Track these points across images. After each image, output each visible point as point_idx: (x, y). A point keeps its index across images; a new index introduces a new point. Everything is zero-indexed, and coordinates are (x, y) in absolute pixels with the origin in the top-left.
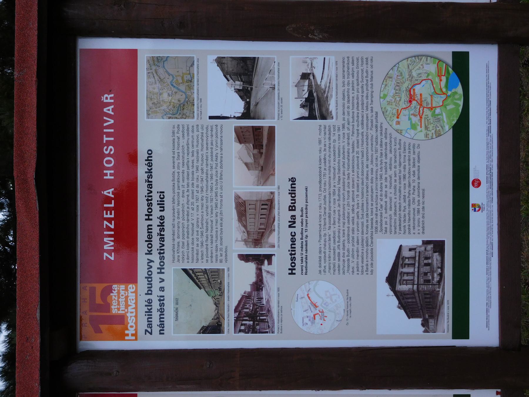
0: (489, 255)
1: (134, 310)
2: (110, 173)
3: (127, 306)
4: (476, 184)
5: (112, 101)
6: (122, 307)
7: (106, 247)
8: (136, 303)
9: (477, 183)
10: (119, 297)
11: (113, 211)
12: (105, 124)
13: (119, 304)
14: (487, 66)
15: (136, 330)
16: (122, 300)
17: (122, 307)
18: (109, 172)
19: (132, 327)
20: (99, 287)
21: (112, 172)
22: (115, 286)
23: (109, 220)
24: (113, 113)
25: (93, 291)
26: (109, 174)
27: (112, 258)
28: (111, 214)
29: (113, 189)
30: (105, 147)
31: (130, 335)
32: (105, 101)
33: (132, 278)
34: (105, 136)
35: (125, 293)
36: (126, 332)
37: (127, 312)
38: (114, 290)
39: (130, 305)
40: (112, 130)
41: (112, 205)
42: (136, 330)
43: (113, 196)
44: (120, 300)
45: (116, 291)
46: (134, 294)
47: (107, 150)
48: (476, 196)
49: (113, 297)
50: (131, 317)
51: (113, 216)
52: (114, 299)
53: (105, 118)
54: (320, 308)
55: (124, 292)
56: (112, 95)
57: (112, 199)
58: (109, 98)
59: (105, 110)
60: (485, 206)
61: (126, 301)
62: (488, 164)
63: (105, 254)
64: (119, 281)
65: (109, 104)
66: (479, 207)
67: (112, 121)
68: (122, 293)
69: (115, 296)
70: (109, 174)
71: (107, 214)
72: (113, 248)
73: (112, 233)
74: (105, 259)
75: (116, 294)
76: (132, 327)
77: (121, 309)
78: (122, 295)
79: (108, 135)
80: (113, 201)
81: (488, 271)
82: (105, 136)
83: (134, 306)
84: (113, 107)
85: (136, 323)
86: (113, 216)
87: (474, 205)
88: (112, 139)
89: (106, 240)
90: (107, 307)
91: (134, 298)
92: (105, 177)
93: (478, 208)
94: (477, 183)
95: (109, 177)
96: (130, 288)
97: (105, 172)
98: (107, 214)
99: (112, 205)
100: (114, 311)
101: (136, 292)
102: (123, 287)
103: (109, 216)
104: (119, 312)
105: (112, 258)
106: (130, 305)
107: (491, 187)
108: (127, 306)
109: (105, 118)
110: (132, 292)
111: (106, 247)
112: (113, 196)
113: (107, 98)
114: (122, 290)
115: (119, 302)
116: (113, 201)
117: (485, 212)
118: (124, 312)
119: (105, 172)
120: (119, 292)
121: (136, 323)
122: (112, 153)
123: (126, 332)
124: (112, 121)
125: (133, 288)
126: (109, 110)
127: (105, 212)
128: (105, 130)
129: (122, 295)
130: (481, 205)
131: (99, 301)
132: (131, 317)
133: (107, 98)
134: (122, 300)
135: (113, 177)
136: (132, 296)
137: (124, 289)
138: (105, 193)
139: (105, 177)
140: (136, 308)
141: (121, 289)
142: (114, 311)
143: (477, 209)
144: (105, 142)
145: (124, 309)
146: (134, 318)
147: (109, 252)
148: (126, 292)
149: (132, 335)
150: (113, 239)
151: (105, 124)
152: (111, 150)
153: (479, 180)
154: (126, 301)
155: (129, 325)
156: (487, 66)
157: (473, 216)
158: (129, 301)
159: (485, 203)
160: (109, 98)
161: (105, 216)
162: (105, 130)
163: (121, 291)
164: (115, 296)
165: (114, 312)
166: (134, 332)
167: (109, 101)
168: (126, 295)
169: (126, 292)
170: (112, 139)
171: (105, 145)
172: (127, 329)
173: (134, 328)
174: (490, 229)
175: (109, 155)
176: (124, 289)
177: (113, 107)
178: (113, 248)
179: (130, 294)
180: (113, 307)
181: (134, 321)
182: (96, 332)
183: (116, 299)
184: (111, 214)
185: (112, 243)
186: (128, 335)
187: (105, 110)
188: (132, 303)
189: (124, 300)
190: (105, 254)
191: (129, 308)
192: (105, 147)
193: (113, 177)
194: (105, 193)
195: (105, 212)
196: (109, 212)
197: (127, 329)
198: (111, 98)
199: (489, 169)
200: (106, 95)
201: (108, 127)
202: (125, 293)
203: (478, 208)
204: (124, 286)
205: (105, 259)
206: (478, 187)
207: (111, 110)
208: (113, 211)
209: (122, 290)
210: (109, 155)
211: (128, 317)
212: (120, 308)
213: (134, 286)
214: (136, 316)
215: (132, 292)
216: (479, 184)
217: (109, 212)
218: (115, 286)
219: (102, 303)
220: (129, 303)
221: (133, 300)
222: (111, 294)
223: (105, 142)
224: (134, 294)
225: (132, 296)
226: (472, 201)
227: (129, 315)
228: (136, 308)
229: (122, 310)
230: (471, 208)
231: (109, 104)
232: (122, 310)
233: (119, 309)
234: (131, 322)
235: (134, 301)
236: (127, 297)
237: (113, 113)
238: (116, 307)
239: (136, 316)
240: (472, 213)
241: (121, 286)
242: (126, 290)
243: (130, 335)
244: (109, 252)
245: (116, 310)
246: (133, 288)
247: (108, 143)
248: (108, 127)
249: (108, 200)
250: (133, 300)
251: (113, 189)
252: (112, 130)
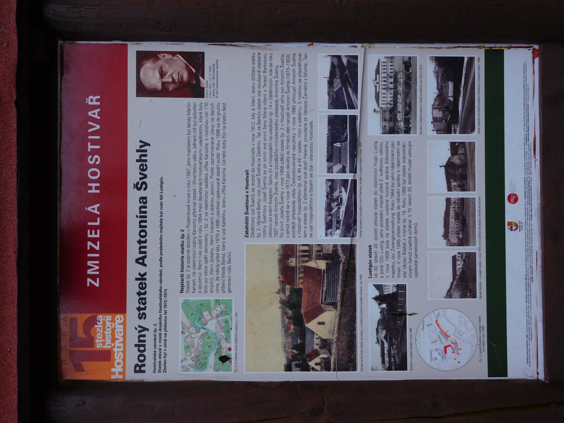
0: (529, 280)
1: (122, 345)
2: (95, 187)
3: (114, 340)
4: (512, 199)
5: (98, 103)
6: (108, 341)
7: (89, 272)
8: (124, 337)
9: (514, 199)
10: (104, 330)
11: (98, 231)
12: (90, 130)
13: (104, 338)
14: (525, 66)
15: (124, 367)
17: (108, 341)
18: (94, 185)
19: (119, 364)
20: (82, 318)
21: (98, 185)
23: (94, 241)
24: (99, 118)
25: (73, 321)
26: (94, 188)
27: (97, 285)
28: (96, 233)
29: (98, 205)
30: (90, 157)
31: (117, 373)
32: (90, 103)
33: (121, 308)
34: (89, 143)
35: (112, 325)
36: (113, 370)
37: (114, 347)
38: (99, 321)
39: (118, 339)
40: (98, 137)
41: (98, 223)
42: (124, 367)
43: (98, 213)
44: (106, 333)
45: (101, 323)
46: (122, 326)
47: (91, 160)
48: (512, 212)
49: (98, 329)
50: (118, 352)
51: (98, 236)
52: (99, 332)
53: (90, 123)
54: (453, 338)
55: (110, 323)
56: (98, 97)
57: (97, 216)
58: (94, 100)
59: (90, 114)
60: (524, 224)
61: (113, 334)
62: (526, 176)
63: (89, 280)
65: (95, 107)
66: (516, 225)
67: (98, 127)
68: (108, 324)
69: (100, 328)
70: (94, 188)
71: (91, 233)
72: (97, 273)
73: (98, 255)
74: (88, 285)
75: (102, 326)
76: (119, 364)
77: (106, 344)
78: (108, 328)
79: (94, 142)
80: (98, 219)
81: (528, 298)
82: (89, 143)
83: (122, 340)
84: (99, 110)
85: (124, 360)
86: (98, 236)
87: (509, 224)
88: (98, 147)
89: (89, 263)
90: (91, 341)
91: (122, 330)
92: (90, 191)
93: (515, 226)
94: (514, 199)
95: (94, 191)
96: (118, 319)
97: (90, 185)
98: (91, 233)
99: (98, 223)
100: (99, 346)
101: (124, 324)
102: (109, 317)
103: (93, 236)
104: (104, 347)
105: (97, 285)
106: (118, 339)
107: (530, 203)
108: (114, 340)
109: (90, 123)
110: (119, 324)
111: (89, 272)
112: (98, 213)
113: (93, 100)
114: (109, 321)
115: (104, 335)
116: (98, 219)
117: (523, 232)
118: (110, 347)
119: (90, 185)
120: (104, 324)
121: (124, 360)
122: (98, 163)
123: (113, 370)
124: (98, 127)
125: (121, 319)
126: (94, 114)
127: (89, 231)
128: (90, 137)
129: (108, 328)
130: (518, 223)
131: (81, 333)
132: (118, 352)
133: (92, 100)
134: (108, 332)
135: (98, 191)
136: (119, 328)
137: (110, 320)
138: (89, 209)
139: (90, 191)
140: (124, 342)
141: (107, 320)
142: (99, 346)
143: (514, 228)
144: (89, 150)
145: (110, 343)
146: (122, 354)
147: (94, 277)
148: (113, 324)
149: (120, 373)
150: (98, 262)
151: (90, 130)
152: (97, 160)
153: (516, 195)
154: (113, 334)
155: (116, 362)
156: (525, 66)
157: (509, 235)
158: (116, 334)
159: (523, 221)
160: (94, 100)
161: (89, 236)
162: (90, 137)
163: (107, 323)
164: (100, 328)
165: (98, 347)
166: (121, 370)
167: (94, 103)
168: (113, 327)
169: (113, 324)
170: (98, 147)
171: (89, 154)
172: (114, 367)
173: (122, 365)
174: (529, 250)
175: (94, 166)
176: (110, 320)
177: (99, 110)
178: (97, 273)
179: (117, 326)
180: (97, 341)
181: (122, 357)
182: (77, 371)
183: (101, 331)
184: (96, 233)
185: (97, 268)
186: (114, 373)
187: (90, 114)
188: (119, 336)
189: (110, 332)
190: (89, 280)
191: (116, 342)
192: (90, 157)
193: (98, 191)
194: (89, 209)
195: (89, 231)
196: (93, 231)
197: (114, 367)
198: (97, 100)
199: (528, 183)
200: (91, 97)
201: (93, 133)
202: (112, 325)
203: (515, 226)
204: (110, 317)
205: (88, 285)
206: (514, 203)
207: (96, 114)
208: (98, 231)
209: (109, 321)
210: (94, 166)
211: (114, 353)
212: (105, 342)
213: (122, 317)
214: (124, 352)
215: (119, 324)
216: (516, 200)
217: (93, 231)
218: (100, 317)
219: (85, 336)
220: (116, 337)
221: (120, 332)
222: (96, 326)
223: (89, 150)
224: (122, 326)
225: (119, 328)
226: (508, 219)
227: (115, 350)
228: (124, 342)
229: (108, 345)
230: (507, 227)
231: (95, 107)
232: (108, 345)
233: (104, 343)
234: (118, 357)
235: (122, 334)
236: (113, 330)
237: (99, 118)
238: (101, 341)
239: (124, 352)
240: (508, 232)
241: (107, 317)
242: (113, 321)
243: (117, 373)
244: (94, 277)
245: (101, 344)
246: (121, 319)
247: (94, 152)
248: (93, 133)
249: (93, 217)
250: (120, 332)
251: (98, 205)
252: (98, 137)
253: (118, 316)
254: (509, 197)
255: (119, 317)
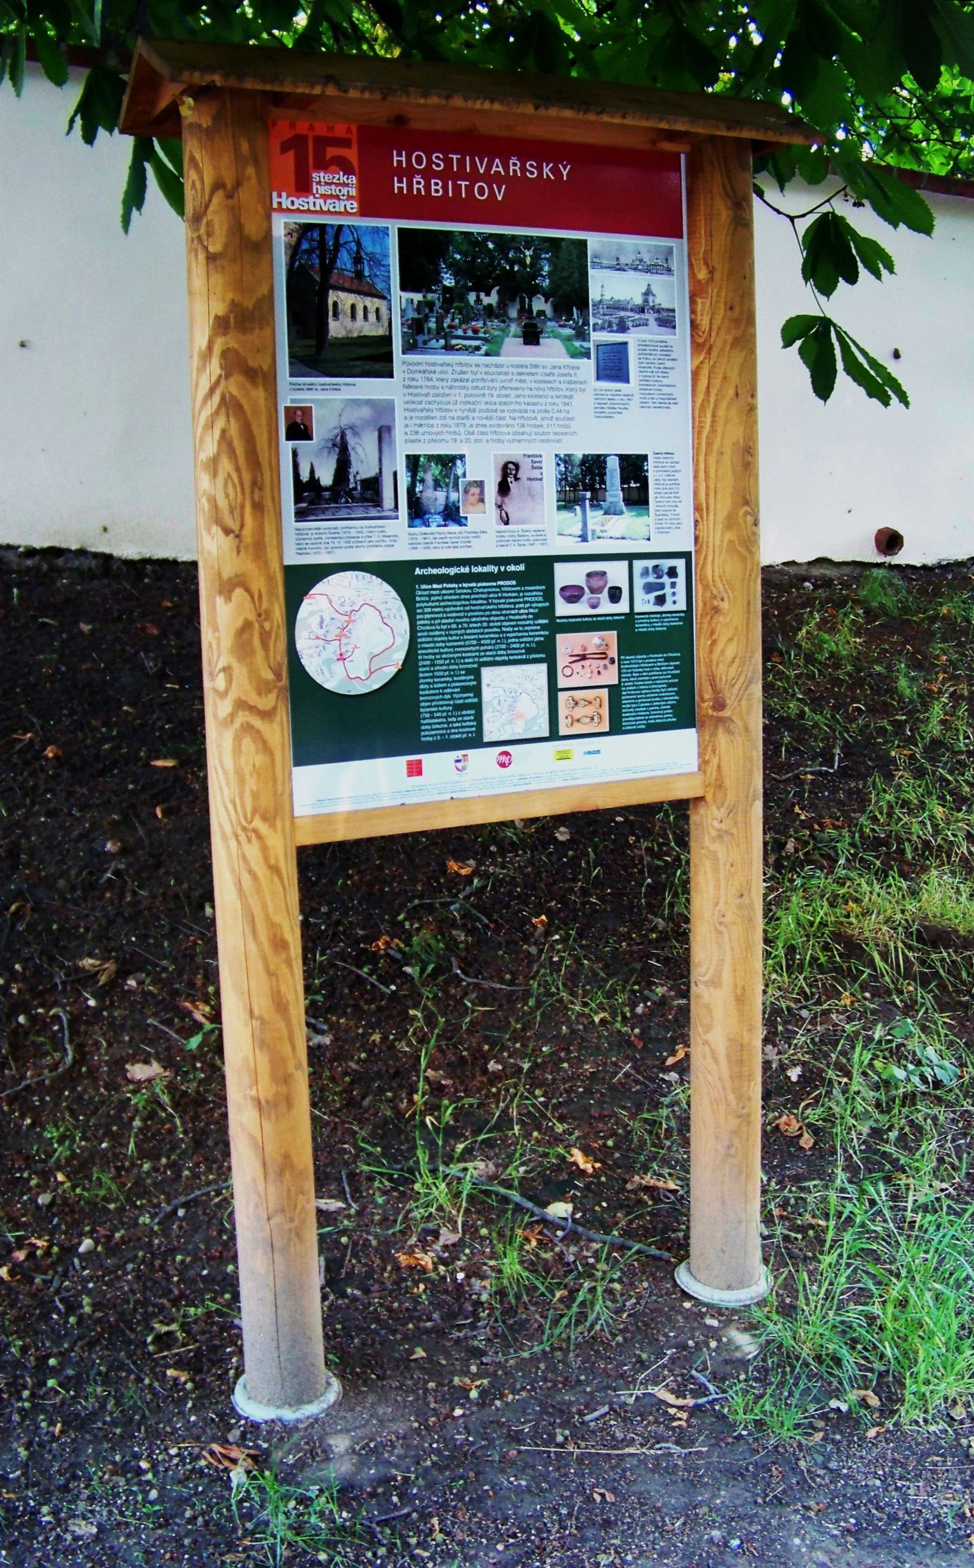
4: (504, 759)
6: (323, 190)
16: (334, 190)
20: (352, 154)
22: (353, 180)
61: (331, 197)
64: (361, 188)
68: (345, 191)
90: (323, 166)
102: (353, 192)
131: (331, 152)
134: (334, 190)
140: (322, 212)
216: (503, 765)
218: (353, 180)
225: (340, 207)
242: (350, 198)
253: (355, 205)
254: (506, 754)
255: (353, 206)
